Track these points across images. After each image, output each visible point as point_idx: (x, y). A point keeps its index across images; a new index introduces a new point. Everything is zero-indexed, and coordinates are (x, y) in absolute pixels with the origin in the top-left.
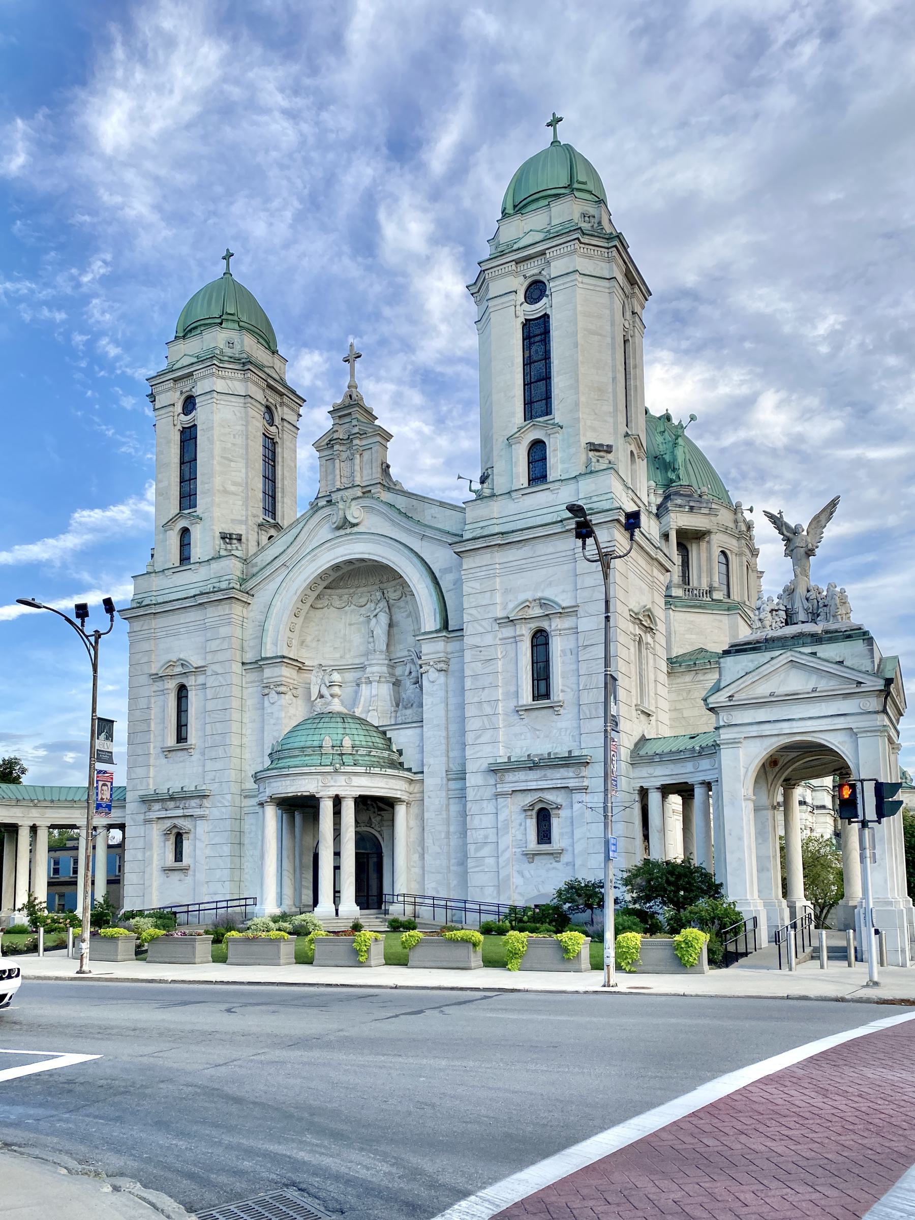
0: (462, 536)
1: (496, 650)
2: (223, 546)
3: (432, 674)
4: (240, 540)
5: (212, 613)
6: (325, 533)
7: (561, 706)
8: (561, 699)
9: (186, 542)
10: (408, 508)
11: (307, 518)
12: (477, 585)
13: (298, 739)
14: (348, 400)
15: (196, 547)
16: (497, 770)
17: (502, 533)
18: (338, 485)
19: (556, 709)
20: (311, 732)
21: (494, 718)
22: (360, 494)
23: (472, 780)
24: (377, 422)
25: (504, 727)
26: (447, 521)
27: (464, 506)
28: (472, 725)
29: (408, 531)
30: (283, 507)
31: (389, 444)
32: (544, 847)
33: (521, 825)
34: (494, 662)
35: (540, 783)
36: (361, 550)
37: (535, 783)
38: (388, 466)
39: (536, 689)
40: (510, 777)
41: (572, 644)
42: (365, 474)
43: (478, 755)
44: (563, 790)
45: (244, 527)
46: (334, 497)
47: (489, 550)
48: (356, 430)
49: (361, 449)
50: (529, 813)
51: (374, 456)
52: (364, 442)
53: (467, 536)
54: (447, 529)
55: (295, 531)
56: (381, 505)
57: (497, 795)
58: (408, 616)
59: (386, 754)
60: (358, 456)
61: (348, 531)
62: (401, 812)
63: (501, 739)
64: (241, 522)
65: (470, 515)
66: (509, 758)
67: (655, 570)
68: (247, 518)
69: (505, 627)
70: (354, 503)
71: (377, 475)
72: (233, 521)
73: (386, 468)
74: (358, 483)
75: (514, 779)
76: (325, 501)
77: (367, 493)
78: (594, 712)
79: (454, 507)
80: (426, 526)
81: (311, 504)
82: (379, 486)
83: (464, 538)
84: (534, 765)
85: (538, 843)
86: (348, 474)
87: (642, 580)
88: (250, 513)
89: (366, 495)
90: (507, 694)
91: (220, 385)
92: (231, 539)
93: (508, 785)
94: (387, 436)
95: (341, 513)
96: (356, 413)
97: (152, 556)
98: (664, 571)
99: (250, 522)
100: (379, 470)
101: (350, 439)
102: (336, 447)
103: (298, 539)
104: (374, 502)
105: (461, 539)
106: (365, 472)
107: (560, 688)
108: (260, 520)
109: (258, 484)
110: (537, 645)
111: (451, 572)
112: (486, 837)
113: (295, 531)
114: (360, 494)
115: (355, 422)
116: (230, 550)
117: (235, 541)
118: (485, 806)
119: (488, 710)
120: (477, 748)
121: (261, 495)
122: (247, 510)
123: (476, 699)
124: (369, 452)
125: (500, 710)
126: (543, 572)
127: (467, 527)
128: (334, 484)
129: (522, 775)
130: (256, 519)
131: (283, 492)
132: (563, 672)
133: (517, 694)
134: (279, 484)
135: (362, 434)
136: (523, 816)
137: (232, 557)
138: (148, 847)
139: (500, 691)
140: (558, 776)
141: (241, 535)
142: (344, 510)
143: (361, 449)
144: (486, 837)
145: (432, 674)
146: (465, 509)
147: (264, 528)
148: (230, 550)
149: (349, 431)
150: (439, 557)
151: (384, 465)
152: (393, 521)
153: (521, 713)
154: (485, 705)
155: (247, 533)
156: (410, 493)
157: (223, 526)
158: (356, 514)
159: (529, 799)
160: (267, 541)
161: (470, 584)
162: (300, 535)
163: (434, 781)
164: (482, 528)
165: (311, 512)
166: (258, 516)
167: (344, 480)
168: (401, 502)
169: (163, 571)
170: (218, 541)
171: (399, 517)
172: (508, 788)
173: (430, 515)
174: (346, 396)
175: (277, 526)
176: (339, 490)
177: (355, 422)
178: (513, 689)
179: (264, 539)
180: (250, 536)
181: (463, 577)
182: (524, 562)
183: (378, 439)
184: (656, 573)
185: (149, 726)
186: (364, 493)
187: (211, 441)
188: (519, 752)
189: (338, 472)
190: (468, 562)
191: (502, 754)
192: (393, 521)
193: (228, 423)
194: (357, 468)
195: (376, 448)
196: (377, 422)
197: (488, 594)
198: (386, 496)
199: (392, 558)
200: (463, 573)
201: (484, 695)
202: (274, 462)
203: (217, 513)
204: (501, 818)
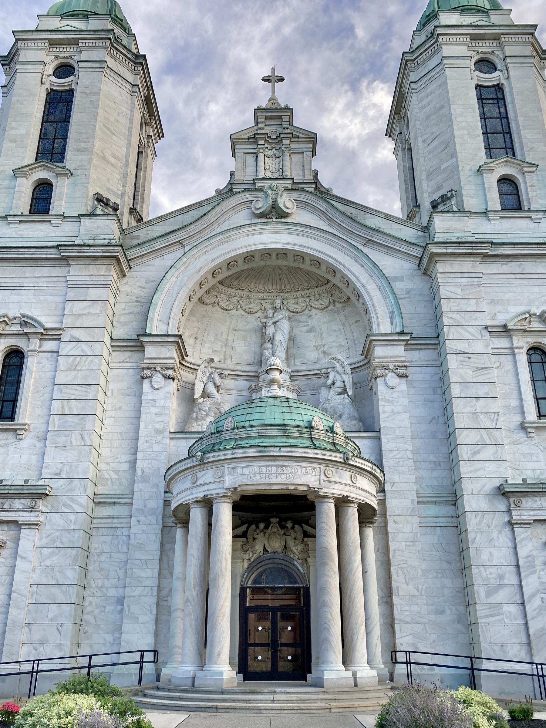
13: (256, 416)
20: (276, 409)
40: (528, 503)
43: (478, 474)
58: (309, 331)
93: (527, 513)
101: (279, 139)
156: (348, 201)
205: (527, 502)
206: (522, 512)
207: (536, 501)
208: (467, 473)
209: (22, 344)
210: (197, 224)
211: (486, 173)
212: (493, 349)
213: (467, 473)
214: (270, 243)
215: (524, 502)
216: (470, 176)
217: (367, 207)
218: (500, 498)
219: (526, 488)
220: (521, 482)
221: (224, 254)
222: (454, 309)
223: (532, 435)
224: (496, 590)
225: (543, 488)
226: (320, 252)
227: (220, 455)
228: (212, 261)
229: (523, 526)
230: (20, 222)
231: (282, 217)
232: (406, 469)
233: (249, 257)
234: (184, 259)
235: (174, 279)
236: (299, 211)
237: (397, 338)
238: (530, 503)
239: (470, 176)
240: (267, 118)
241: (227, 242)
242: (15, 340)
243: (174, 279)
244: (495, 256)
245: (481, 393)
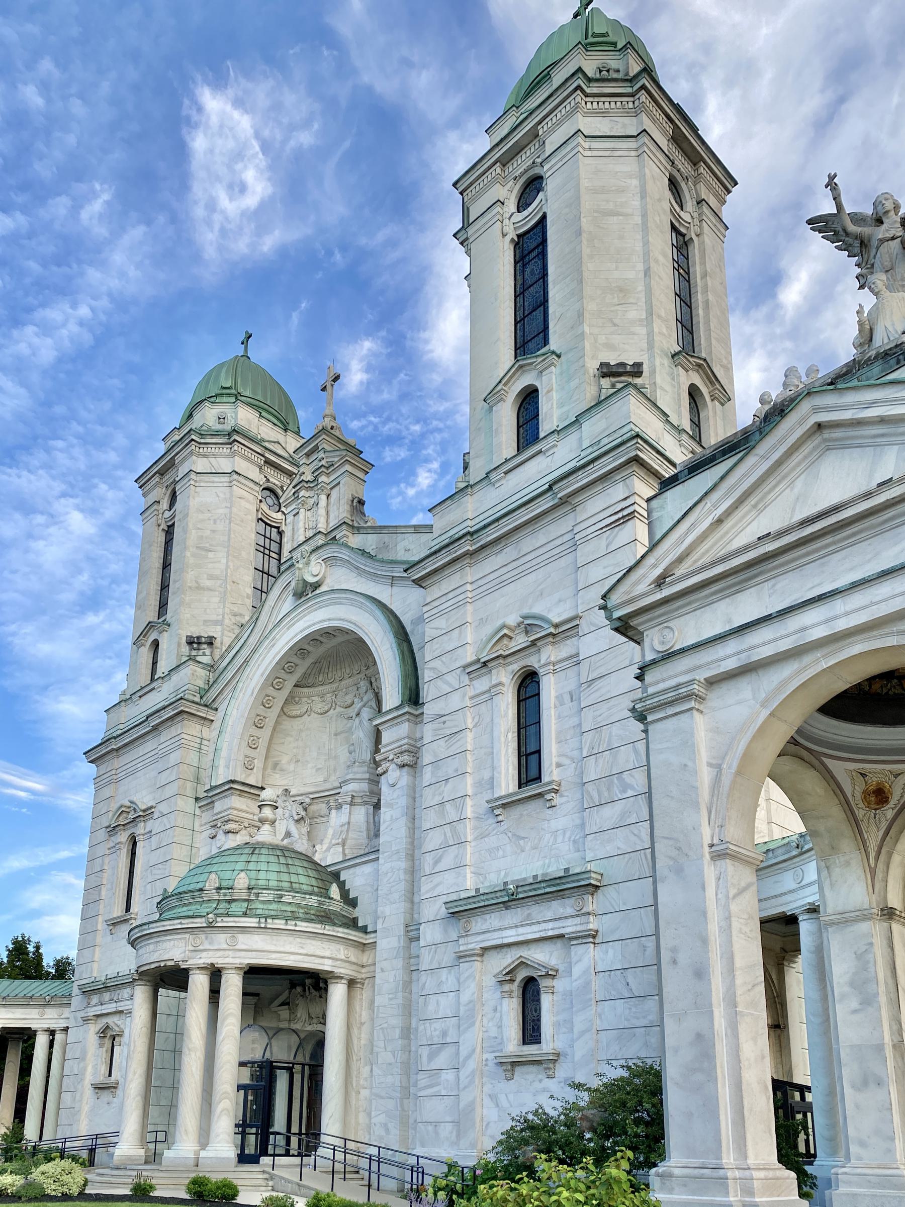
1: (465, 716)
3: (394, 773)
5: (166, 735)
7: (556, 791)
8: (555, 778)
16: (461, 912)
19: (548, 797)
21: (459, 826)
23: (430, 934)
25: (475, 839)
28: (433, 840)
29: (374, 577)
32: (531, 1050)
33: (495, 1010)
34: (458, 736)
35: (521, 930)
37: (512, 932)
39: (523, 770)
40: (479, 924)
41: (571, 685)
44: (559, 943)
50: (507, 987)
57: (461, 957)
59: (313, 901)
62: (337, 992)
63: (468, 859)
66: (477, 890)
69: (479, 677)
75: (484, 927)
78: (606, 794)
84: (511, 898)
85: (524, 1043)
90: (479, 784)
91: (200, 464)
107: (554, 760)
110: (525, 699)
112: (444, 1034)
118: (444, 979)
119: (451, 813)
120: (437, 879)
123: (437, 799)
125: (469, 812)
129: (493, 920)
132: (559, 733)
133: (491, 783)
136: (498, 995)
138: (82, 1058)
139: (469, 780)
140: (549, 915)
144: (444, 1034)
145: (394, 773)
152: (357, 568)
153: (497, 812)
154: (448, 806)
159: (507, 959)
163: (388, 942)
172: (474, 943)
178: (486, 775)
185: (100, 894)
187: (185, 531)
188: (493, 880)
191: (469, 883)
192: (357, 568)
199: (353, 618)
201: (448, 791)
204: (465, 997)
205: (477, 922)
206: (469, 938)
207: (486, 920)
208: (427, 892)
209: (533, 661)
210: (254, 633)
212: (471, 698)
213: (427, 892)
215: (474, 924)
218: (453, 920)
219: (467, 904)
220: (473, 893)
222: (436, 654)
223: (500, 818)
224: (438, 1051)
225: (485, 900)
226: (343, 620)
227: (230, 922)
229: (468, 959)
230: (140, 697)
231: (316, 588)
232: (396, 896)
237: (395, 714)
238: (479, 924)
240: (308, 455)
242: (523, 658)
244: (483, 547)
245: (451, 773)
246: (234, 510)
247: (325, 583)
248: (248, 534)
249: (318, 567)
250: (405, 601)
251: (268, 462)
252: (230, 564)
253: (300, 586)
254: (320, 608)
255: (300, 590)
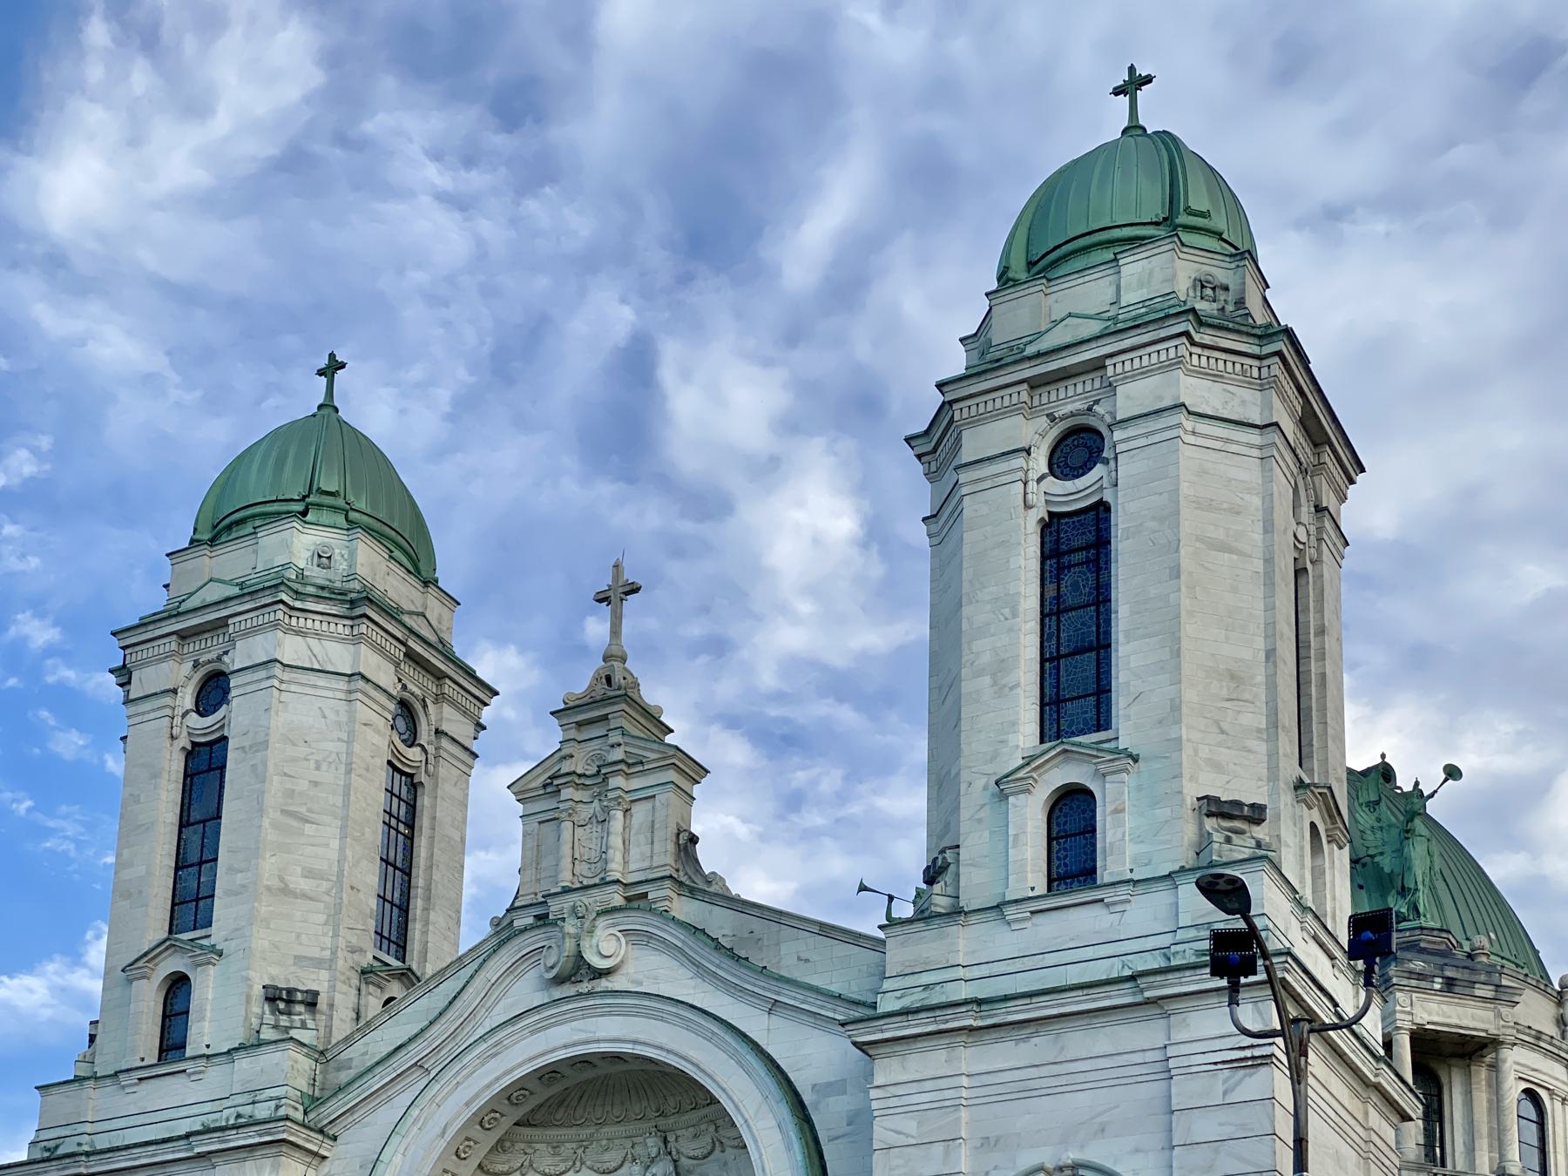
0: (874, 1006)
2: (269, 1018)
4: (311, 1003)
6: (526, 991)
9: (177, 1008)
10: (740, 942)
11: (483, 954)
12: (910, 1125)
14: (601, 688)
15: (202, 1019)
17: (979, 1002)
18: (566, 879)
22: (618, 900)
24: (669, 739)
26: (838, 973)
27: (881, 935)
30: (425, 933)
31: (696, 790)
36: (614, 1034)
38: (694, 840)
42: (632, 850)
45: (324, 975)
46: (555, 906)
47: (944, 1041)
48: (618, 754)
49: (628, 798)
51: (660, 815)
52: (636, 783)
53: (887, 1004)
54: (835, 988)
55: (450, 987)
56: (672, 928)
60: (619, 814)
61: (585, 987)
64: (318, 963)
65: (898, 955)
67: (1372, 1112)
68: (334, 953)
70: (602, 922)
71: (665, 857)
72: (298, 959)
73: (687, 844)
74: (618, 876)
76: (530, 916)
77: (636, 900)
79: (856, 938)
80: (781, 979)
81: (496, 923)
82: (668, 883)
83: (880, 1010)
86: (594, 855)
87: (1342, 1134)
88: (342, 943)
89: (635, 904)
92: (289, 1002)
94: (695, 771)
95: (569, 945)
96: (621, 717)
97: (92, 1038)
98: (1395, 1119)
99: (341, 963)
100: (671, 847)
102: (567, 793)
103: (458, 1004)
104: (655, 920)
105: (870, 1012)
106: (634, 852)
108: (367, 960)
109: (369, 876)
111: (844, 1093)
113: (450, 987)
114: (618, 900)
115: (615, 737)
116: (287, 1029)
117: (300, 1008)
121: (373, 903)
122: (336, 935)
124: (647, 805)
126: (1083, 1100)
127: (887, 985)
128: (555, 878)
130: (356, 956)
131: (428, 899)
134: (419, 880)
135: (632, 765)
137: (290, 1045)
141: (316, 994)
142: (578, 938)
143: (628, 798)
146: (883, 942)
147: (373, 978)
148: (287, 1029)
149: (600, 757)
150: (814, 1055)
151: (684, 837)
155: (333, 988)
157: (274, 970)
158: (608, 947)
160: (380, 1009)
161: (889, 1122)
162: (465, 996)
164: (926, 987)
165: (495, 941)
166: (362, 951)
167: (581, 868)
168: (720, 923)
169: (116, 1074)
170: (258, 1007)
171: (715, 957)
173: (788, 956)
174: (596, 679)
175: (407, 977)
176: (567, 891)
177: (615, 737)
179: (373, 1004)
180: (338, 998)
181: (875, 1105)
182: (1034, 1072)
183: (672, 775)
184: (1375, 1120)
186: (628, 899)
189: (566, 849)
190: (888, 1070)
193: (310, 726)
194: (616, 841)
195: (667, 797)
196: (669, 739)
197: (938, 1149)
198: (685, 908)
199: (693, 1054)
200: (873, 1094)
202: (411, 827)
203: (261, 940)
211: (1013, 794)
214: (574, 1045)
216: (983, 806)
217: (781, 913)
221: (488, 1086)
226: (668, 1051)
228: (467, 1104)
233: (549, 1074)
234: (415, 1112)
235: (398, 1158)
236: (635, 952)
239: (983, 806)
241: (494, 1055)
243: (398, 1158)
246: (357, 747)
247: (623, 971)
248: (372, 796)
249: (614, 943)
250: (814, 1055)
251: (411, 655)
252: (349, 853)
253: (570, 965)
254: (610, 1014)
255: (566, 973)
